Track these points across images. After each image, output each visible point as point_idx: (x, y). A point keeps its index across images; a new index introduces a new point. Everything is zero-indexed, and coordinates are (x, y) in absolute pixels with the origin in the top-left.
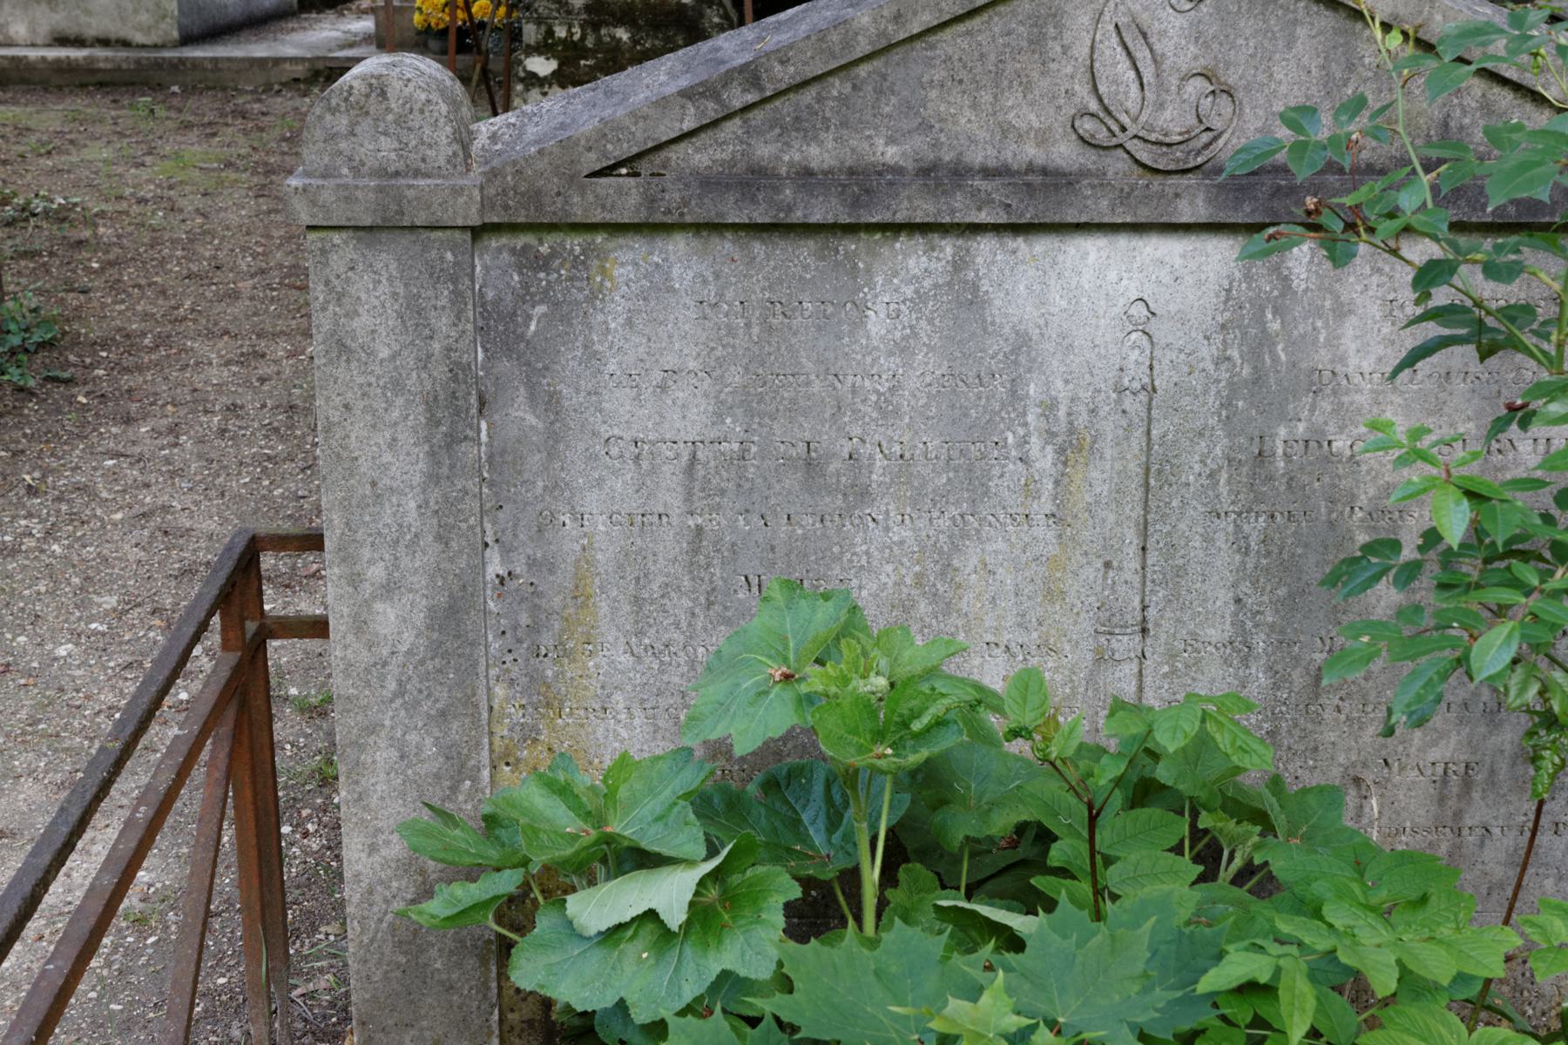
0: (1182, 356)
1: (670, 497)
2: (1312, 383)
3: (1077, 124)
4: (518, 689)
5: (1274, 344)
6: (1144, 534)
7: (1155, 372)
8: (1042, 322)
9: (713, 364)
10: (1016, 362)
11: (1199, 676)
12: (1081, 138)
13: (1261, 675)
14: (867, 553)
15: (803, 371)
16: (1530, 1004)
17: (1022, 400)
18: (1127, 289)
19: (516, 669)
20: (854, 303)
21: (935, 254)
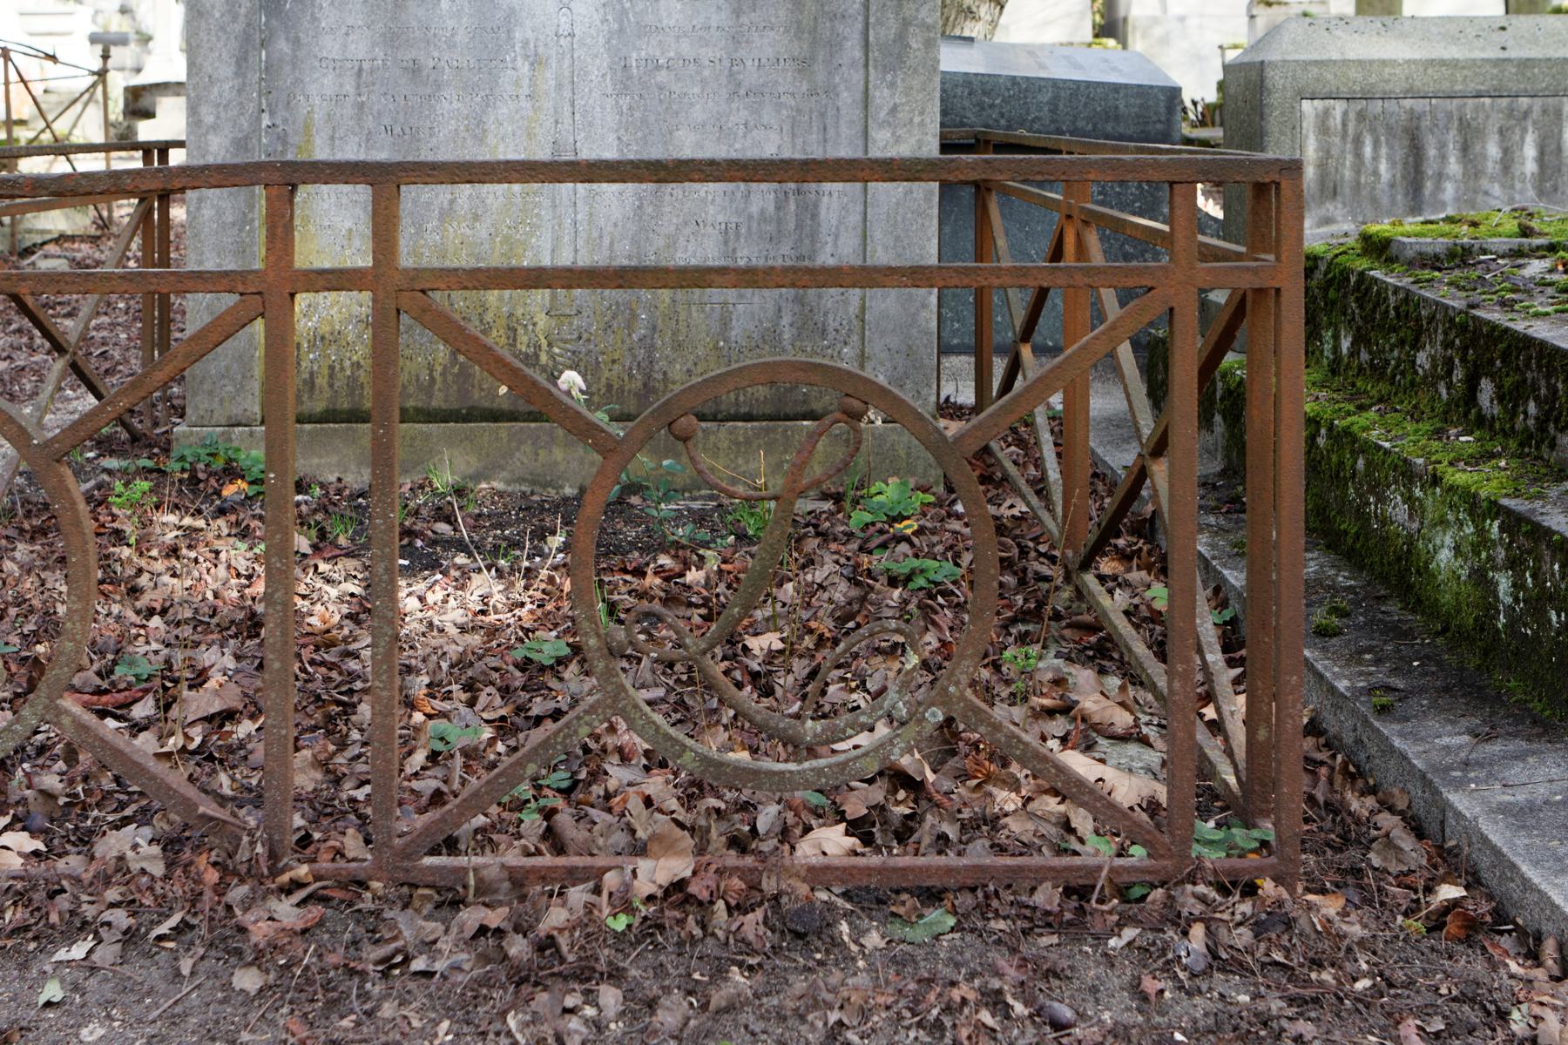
1: (349, 88)
6: (573, 105)
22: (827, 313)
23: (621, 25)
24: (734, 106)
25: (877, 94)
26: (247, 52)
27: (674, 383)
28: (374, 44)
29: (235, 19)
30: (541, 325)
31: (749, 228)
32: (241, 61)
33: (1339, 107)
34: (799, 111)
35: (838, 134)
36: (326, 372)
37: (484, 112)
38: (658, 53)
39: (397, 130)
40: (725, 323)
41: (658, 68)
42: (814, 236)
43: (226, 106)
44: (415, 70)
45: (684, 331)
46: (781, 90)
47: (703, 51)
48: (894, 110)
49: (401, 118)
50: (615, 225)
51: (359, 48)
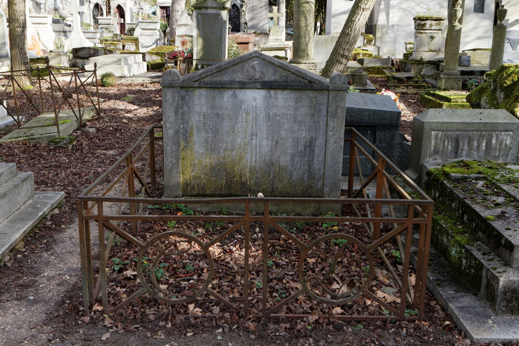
1: (202, 119)
28: (208, 108)
29: (174, 102)
32: (176, 112)
33: (440, 133)
34: (311, 127)
39: (214, 129)
40: (291, 176)
41: (277, 116)
44: (218, 115)
47: (288, 112)
48: (334, 127)
51: (204, 109)
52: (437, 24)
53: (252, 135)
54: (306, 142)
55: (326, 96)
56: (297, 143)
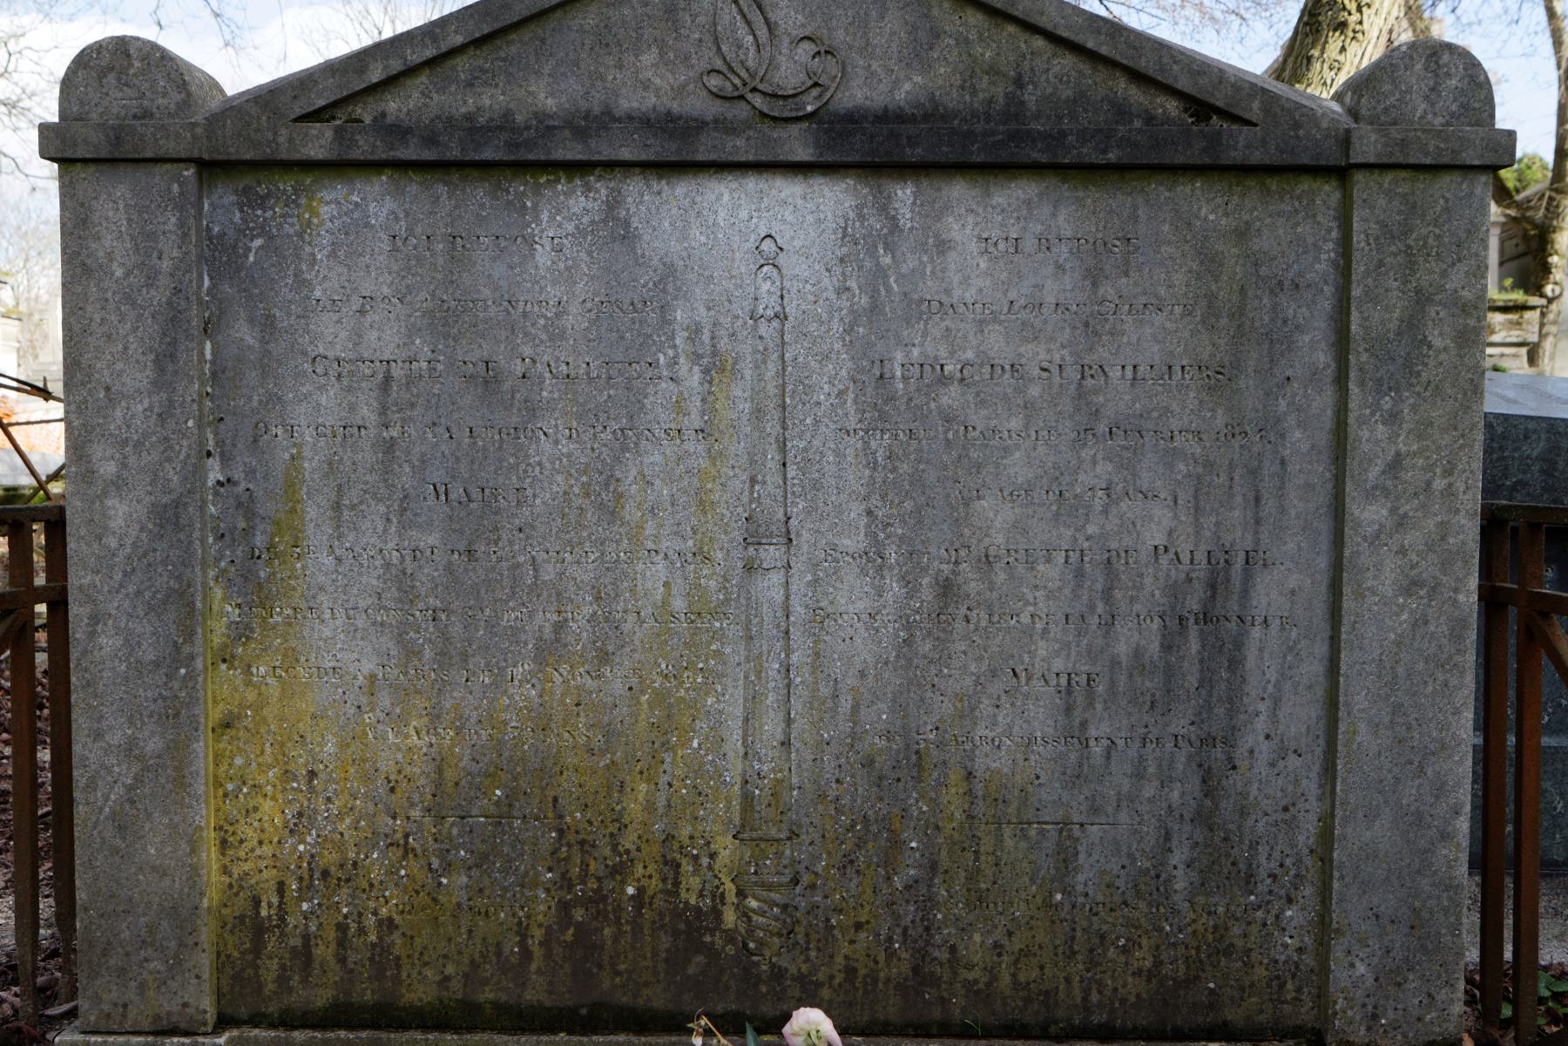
0: (808, 287)
1: (367, 413)
2: (922, 313)
3: (705, 78)
4: (236, 589)
5: (887, 276)
6: (783, 448)
7: (785, 301)
8: (685, 254)
9: (404, 290)
10: (664, 291)
11: (839, 585)
12: (712, 93)
13: (895, 585)
14: (540, 464)
15: (482, 297)
16: (1167, 920)
17: (670, 324)
18: (757, 226)
19: (233, 569)
20: (524, 237)
21: (592, 195)
22: (1254, 845)
23: (874, 295)
24: (1086, 454)
25: (1365, 434)
26: (174, 342)
27: (970, 967)
28: (412, 331)
29: (151, 280)
30: (724, 856)
31: (1113, 684)
32: (165, 360)
34: (1209, 465)
35: (1283, 510)
36: (332, 935)
37: (617, 459)
38: (943, 353)
39: (457, 492)
40: (1066, 859)
41: (944, 380)
42: (1233, 701)
43: (138, 444)
44: (488, 379)
45: (989, 872)
46: (1175, 424)
47: (1027, 349)
48: (1395, 465)
49: (463, 468)
50: (862, 674)
52: (1510, 322)
53: (754, 537)
54: (1174, 591)
55: (1327, 219)
56: (1107, 595)
